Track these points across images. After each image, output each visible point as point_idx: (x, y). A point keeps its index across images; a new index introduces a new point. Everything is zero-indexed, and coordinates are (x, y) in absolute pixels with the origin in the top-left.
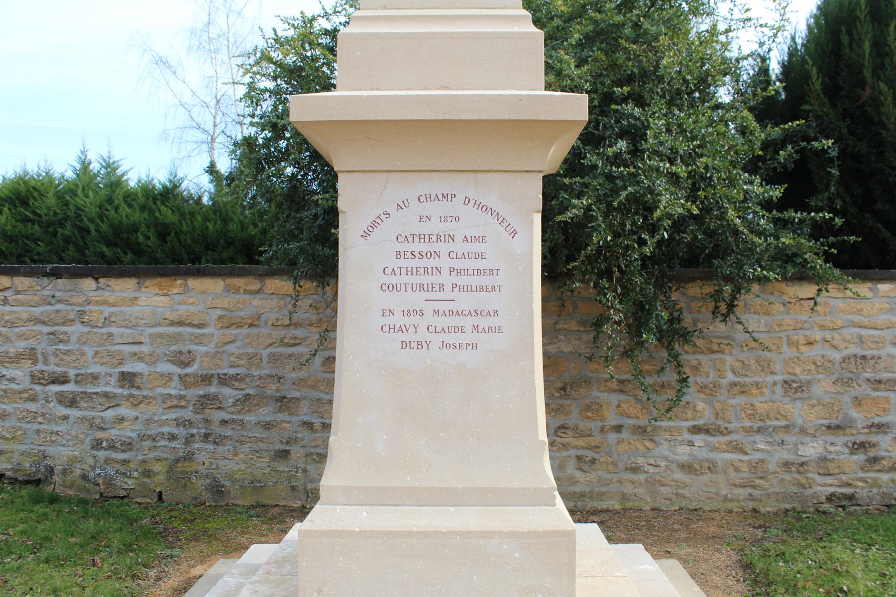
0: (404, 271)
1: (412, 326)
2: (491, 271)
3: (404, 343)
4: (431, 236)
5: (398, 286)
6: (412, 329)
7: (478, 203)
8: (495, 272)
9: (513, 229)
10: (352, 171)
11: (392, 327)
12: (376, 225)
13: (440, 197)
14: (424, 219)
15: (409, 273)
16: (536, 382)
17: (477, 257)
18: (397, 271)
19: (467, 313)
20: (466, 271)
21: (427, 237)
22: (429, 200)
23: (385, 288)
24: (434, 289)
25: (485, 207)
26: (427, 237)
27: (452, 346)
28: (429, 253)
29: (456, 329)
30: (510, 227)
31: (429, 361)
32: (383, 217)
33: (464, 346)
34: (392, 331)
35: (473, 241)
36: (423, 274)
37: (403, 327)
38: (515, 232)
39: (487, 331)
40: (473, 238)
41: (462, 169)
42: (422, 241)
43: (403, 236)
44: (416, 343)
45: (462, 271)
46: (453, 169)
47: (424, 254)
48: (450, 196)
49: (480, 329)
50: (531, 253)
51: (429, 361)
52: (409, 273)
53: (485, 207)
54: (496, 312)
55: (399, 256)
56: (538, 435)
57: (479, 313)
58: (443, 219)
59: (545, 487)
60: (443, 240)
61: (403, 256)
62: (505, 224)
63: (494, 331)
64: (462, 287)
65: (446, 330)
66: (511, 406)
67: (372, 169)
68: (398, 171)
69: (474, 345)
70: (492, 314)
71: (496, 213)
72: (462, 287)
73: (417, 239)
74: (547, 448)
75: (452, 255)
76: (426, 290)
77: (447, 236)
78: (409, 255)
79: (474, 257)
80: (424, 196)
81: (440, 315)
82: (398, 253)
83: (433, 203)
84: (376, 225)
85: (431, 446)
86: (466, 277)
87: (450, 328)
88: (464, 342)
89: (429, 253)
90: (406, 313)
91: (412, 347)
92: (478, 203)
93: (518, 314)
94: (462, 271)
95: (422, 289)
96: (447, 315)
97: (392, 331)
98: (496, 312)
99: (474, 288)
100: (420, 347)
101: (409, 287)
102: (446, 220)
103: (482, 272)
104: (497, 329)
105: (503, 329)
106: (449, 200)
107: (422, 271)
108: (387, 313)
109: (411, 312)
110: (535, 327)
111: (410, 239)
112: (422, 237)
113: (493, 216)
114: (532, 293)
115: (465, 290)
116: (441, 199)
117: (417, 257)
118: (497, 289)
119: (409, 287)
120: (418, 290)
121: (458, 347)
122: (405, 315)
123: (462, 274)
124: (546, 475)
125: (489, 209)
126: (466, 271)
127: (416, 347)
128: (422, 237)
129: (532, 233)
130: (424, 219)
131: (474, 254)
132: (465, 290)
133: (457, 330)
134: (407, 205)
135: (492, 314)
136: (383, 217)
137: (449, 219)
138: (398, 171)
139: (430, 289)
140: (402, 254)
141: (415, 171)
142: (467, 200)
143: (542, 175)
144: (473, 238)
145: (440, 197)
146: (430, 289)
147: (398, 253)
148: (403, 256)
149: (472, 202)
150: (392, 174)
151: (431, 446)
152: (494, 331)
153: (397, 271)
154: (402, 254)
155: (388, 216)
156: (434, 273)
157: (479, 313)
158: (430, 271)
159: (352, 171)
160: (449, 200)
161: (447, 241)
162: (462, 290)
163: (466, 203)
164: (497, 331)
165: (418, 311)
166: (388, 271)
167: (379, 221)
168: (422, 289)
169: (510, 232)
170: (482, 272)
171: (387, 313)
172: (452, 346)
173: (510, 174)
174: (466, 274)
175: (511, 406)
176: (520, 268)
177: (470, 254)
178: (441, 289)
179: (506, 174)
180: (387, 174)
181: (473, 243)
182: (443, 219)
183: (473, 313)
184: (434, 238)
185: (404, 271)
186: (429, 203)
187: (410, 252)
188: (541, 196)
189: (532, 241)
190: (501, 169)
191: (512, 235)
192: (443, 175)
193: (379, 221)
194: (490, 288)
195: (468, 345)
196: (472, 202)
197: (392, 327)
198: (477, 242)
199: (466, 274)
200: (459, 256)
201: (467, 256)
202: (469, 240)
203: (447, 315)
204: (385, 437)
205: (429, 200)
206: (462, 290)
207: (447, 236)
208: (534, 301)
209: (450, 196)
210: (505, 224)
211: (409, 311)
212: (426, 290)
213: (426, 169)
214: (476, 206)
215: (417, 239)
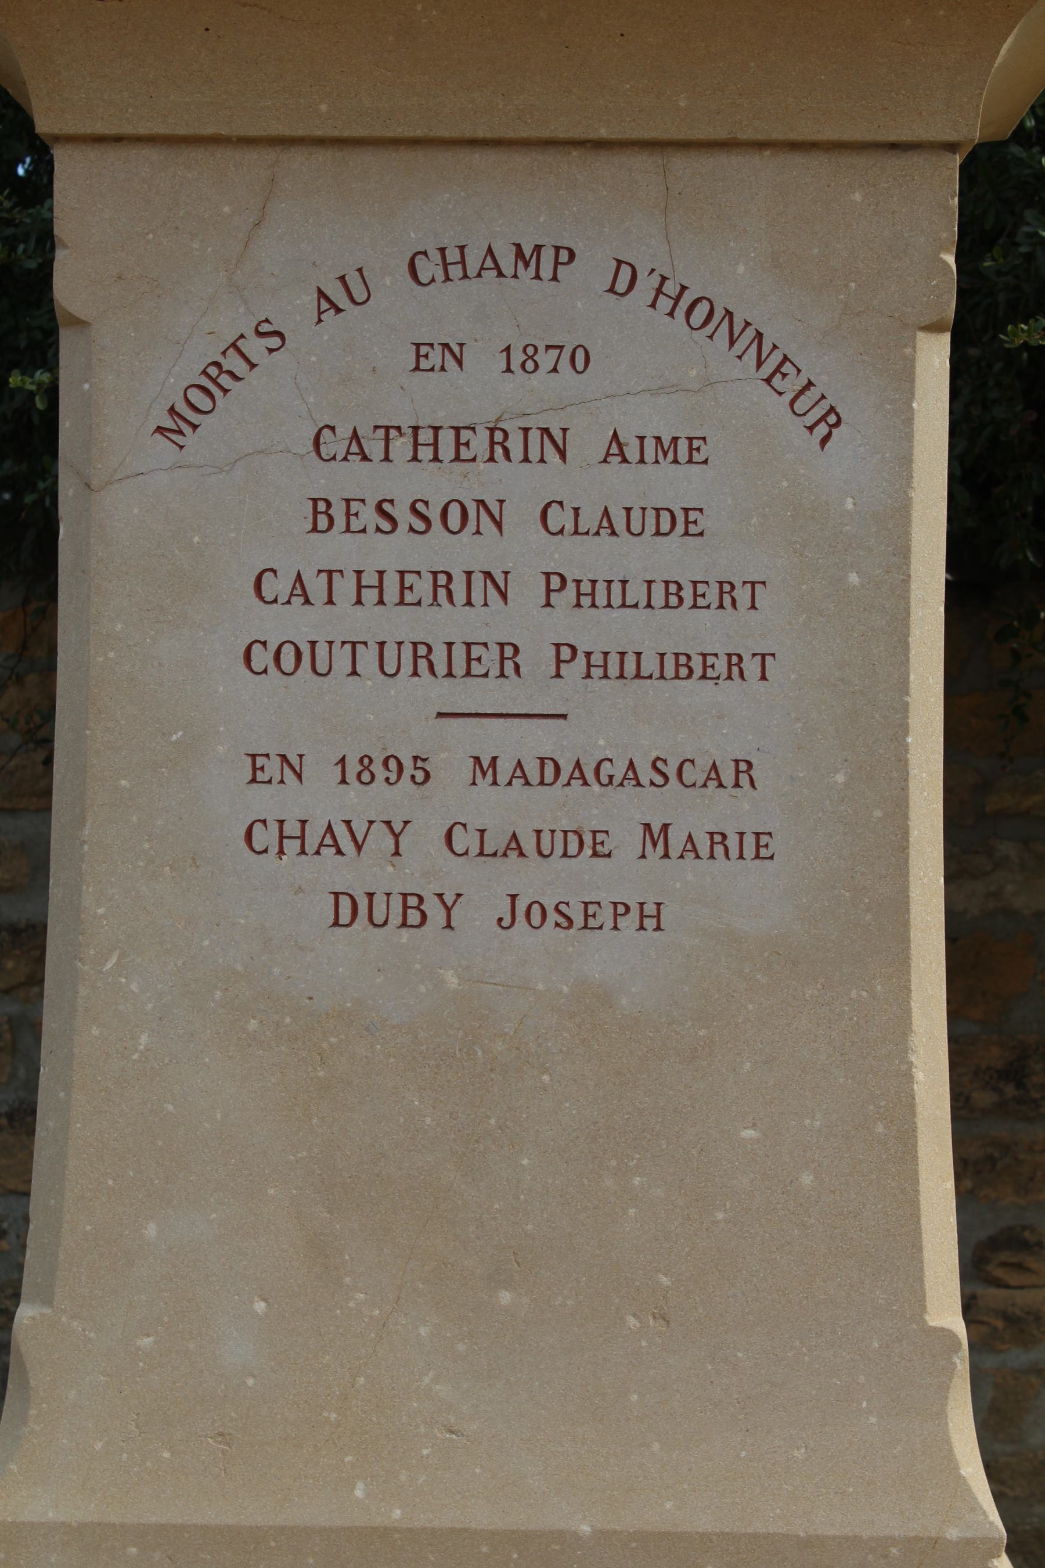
0: (344, 587)
1: (379, 828)
2: (727, 588)
3: (345, 903)
4: (464, 436)
5: (322, 651)
6: (380, 841)
7: (672, 289)
8: (743, 595)
9: (824, 406)
10: (118, 139)
11: (292, 828)
12: (225, 380)
13: (507, 263)
14: (435, 357)
15: (370, 596)
16: (919, 1075)
17: (665, 527)
18: (317, 587)
19: (619, 770)
20: (616, 588)
21: (447, 438)
22: (455, 271)
23: (261, 658)
24: (476, 668)
25: (702, 309)
26: (447, 438)
27: (553, 917)
28: (454, 511)
29: (573, 839)
30: (813, 394)
31: (452, 979)
32: (254, 347)
33: (606, 916)
34: (292, 847)
35: (649, 454)
36: (428, 599)
37: (340, 831)
38: (833, 419)
39: (704, 850)
40: (650, 445)
41: (603, 133)
42: (426, 453)
43: (344, 432)
44: (396, 903)
45: (601, 587)
46: (562, 134)
47: (434, 514)
48: (548, 255)
49: (676, 841)
50: (903, 512)
51: (452, 979)
52: (370, 596)
53: (702, 309)
54: (744, 767)
55: (323, 522)
56: (923, 1308)
57: (671, 771)
58: (518, 357)
59: (953, 1533)
60: (517, 453)
61: (340, 522)
62: (791, 385)
63: (734, 852)
64: (597, 659)
65: (528, 844)
66: (807, 1179)
67: (210, 130)
68: (321, 142)
69: (650, 909)
70: (728, 776)
71: (750, 333)
72: (597, 659)
73: (401, 446)
74: (962, 1364)
75: (557, 518)
76: (441, 669)
77: (534, 436)
78: (368, 516)
79: (651, 528)
80: (436, 257)
81: (502, 779)
82: (320, 507)
83: (473, 285)
84: (225, 380)
85: (461, 1347)
86: (615, 614)
87: (546, 837)
88: (605, 898)
89: (454, 511)
90: (353, 768)
91: (379, 918)
92: (672, 289)
93: (840, 778)
94: (601, 587)
95: (423, 664)
96: (534, 778)
97: (292, 847)
98: (744, 767)
99: (650, 665)
100: (414, 917)
101: (368, 658)
102: (530, 363)
103: (687, 594)
104: (749, 841)
105: (775, 845)
106: (546, 272)
107: (423, 587)
108: (272, 768)
109: (377, 768)
110: (914, 834)
111: (375, 448)
112: (426, 436)
113: (738, 347)
114: (903, 686)
115: (613, 670)
116: (508, 270)
117: (403, 527)
118: (751, 667)
119: (368, 658)
120: (407, 668)
121: (579, 920)
122: (351, 777)
123: (601, 600)
124: (961, 1480)
125: (719, 314)
126: (616, 588)
127: (396, 919)
128: (426, 436)
129: (909, 421)
130: (435, 357)
131: (651, 515)
132: (613, 670)
133: (573, 847)
134: (360, 295)
135: (728, 778)
136: (254, 347)
137: (546, 360)
138: (321, 142)
139: (459, 668)
140: (338, 511)
141: (396, 142)
142: (625, 273)
143: (958, 160)
144: (650, 445)
145: (507, 263)
146: (459, 668)
147: (320, 507)
148: (340, 522)
149: (646, 285)
150: (296, 159)
151: (461, 1347)
152: (734, 852)
153: (317, 587)
154: (338, 511)
155: (275, 342)
156: (477, 597)
157: (671, 771)
158: (459, 588)
159: (118, 139)
160: (546, 272)
161: (534, 454)
162: (597, 672)
163: (621, 286)
164: (749, 850)
165: (408, 764)
166: (278, 586)
167: (238, 366)
168: (423, 664)
169: (810, 419)
170: (687, 594)
171: (272, 768)
172: (553, 917)
173: (816, 162)
174: (616, 601)
175: (807, 1179)
176: (854, 578)
177: (636, 514)
178: (509, 666)
179: (798, 159)
180: (270, 155)
181: (649, 469)
182: (518, 357)
183: (646, 774)
184: (479, 443)
185: (344, 587)
186: (457, 286)
187: (372, 503)
188: (951, 259)
189: (905, 461)
190: (777, 135)
191: (822, 430)
192: (520, 160)
193: (238, 366)
194: (721, 666)
195: (621, 909)
196: (646, 285)
197: (292, 828)
198: (665, 464)
199: (616, 601)
200: (589, 520)
201: (620, 525)
202: (632, 453)
203: (534, 778)
204: (260, 1306)
205: (455, 271)
206: (597, 672)
207: (534, 436)
208: (914, 722)
209: (548, 255)
210: (791, 385)
211: (366, 762)
212: (441, 669)
213: (445, 133)
214: (665, 304)
215: (401, 446)
